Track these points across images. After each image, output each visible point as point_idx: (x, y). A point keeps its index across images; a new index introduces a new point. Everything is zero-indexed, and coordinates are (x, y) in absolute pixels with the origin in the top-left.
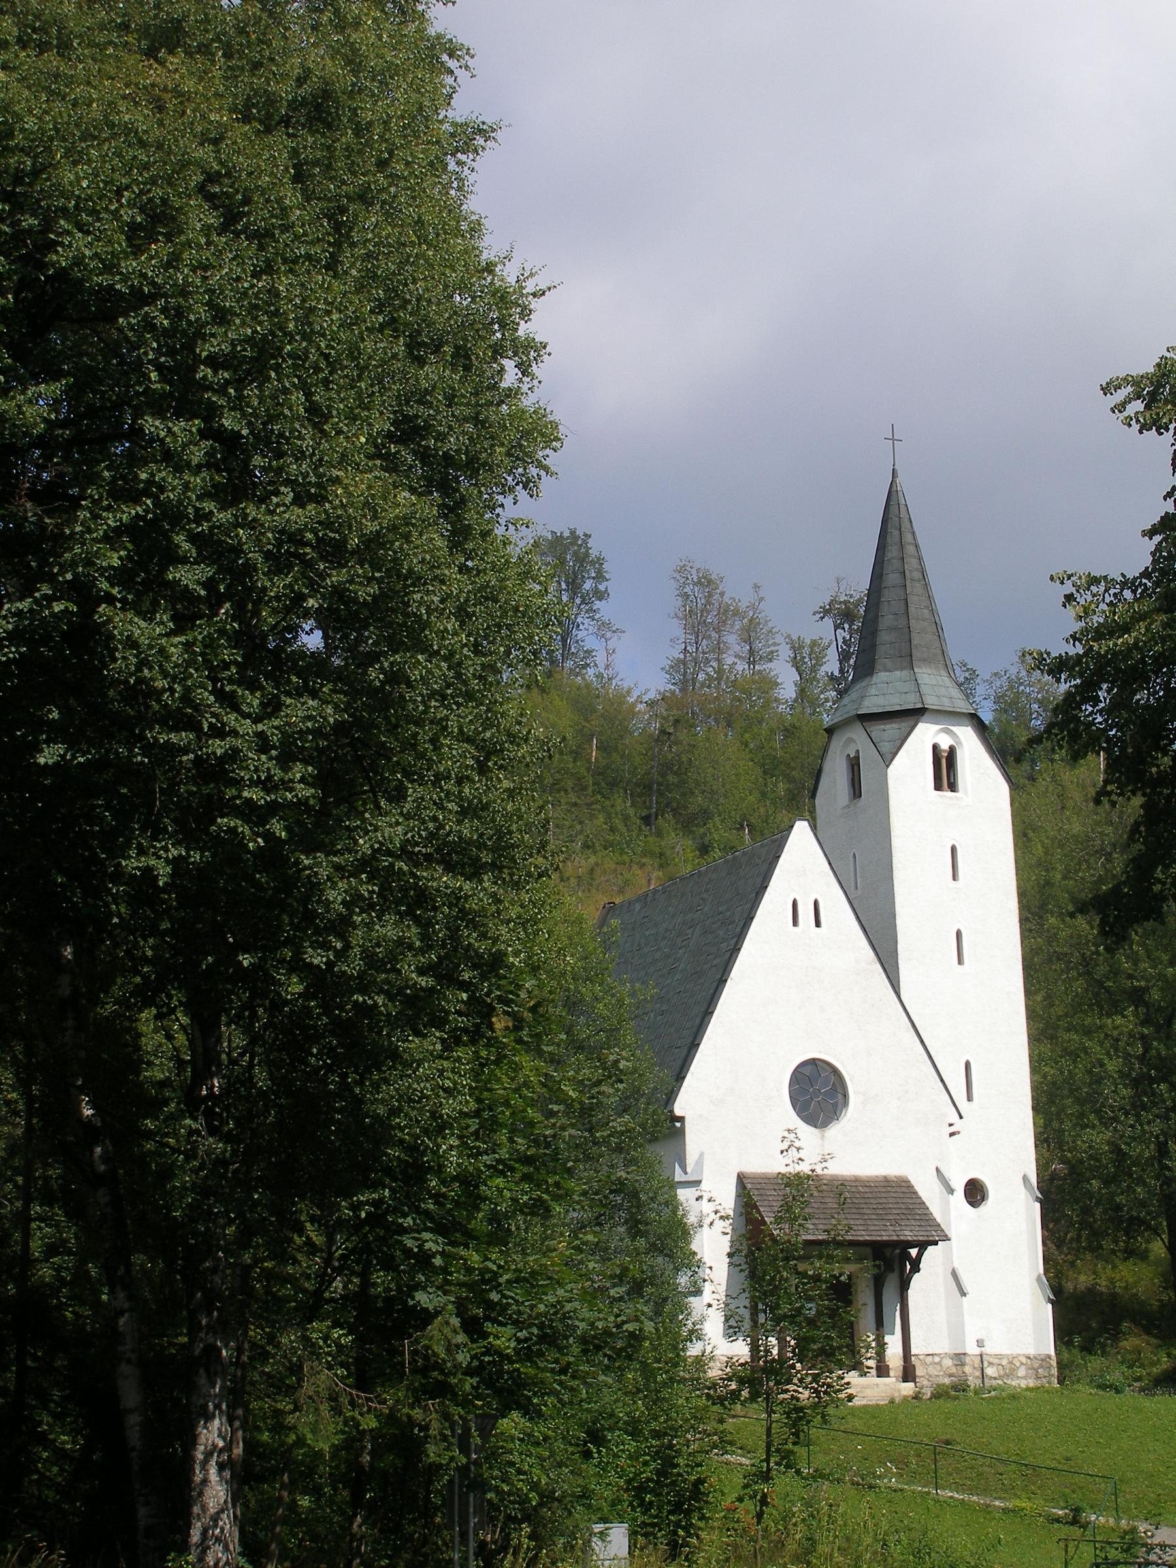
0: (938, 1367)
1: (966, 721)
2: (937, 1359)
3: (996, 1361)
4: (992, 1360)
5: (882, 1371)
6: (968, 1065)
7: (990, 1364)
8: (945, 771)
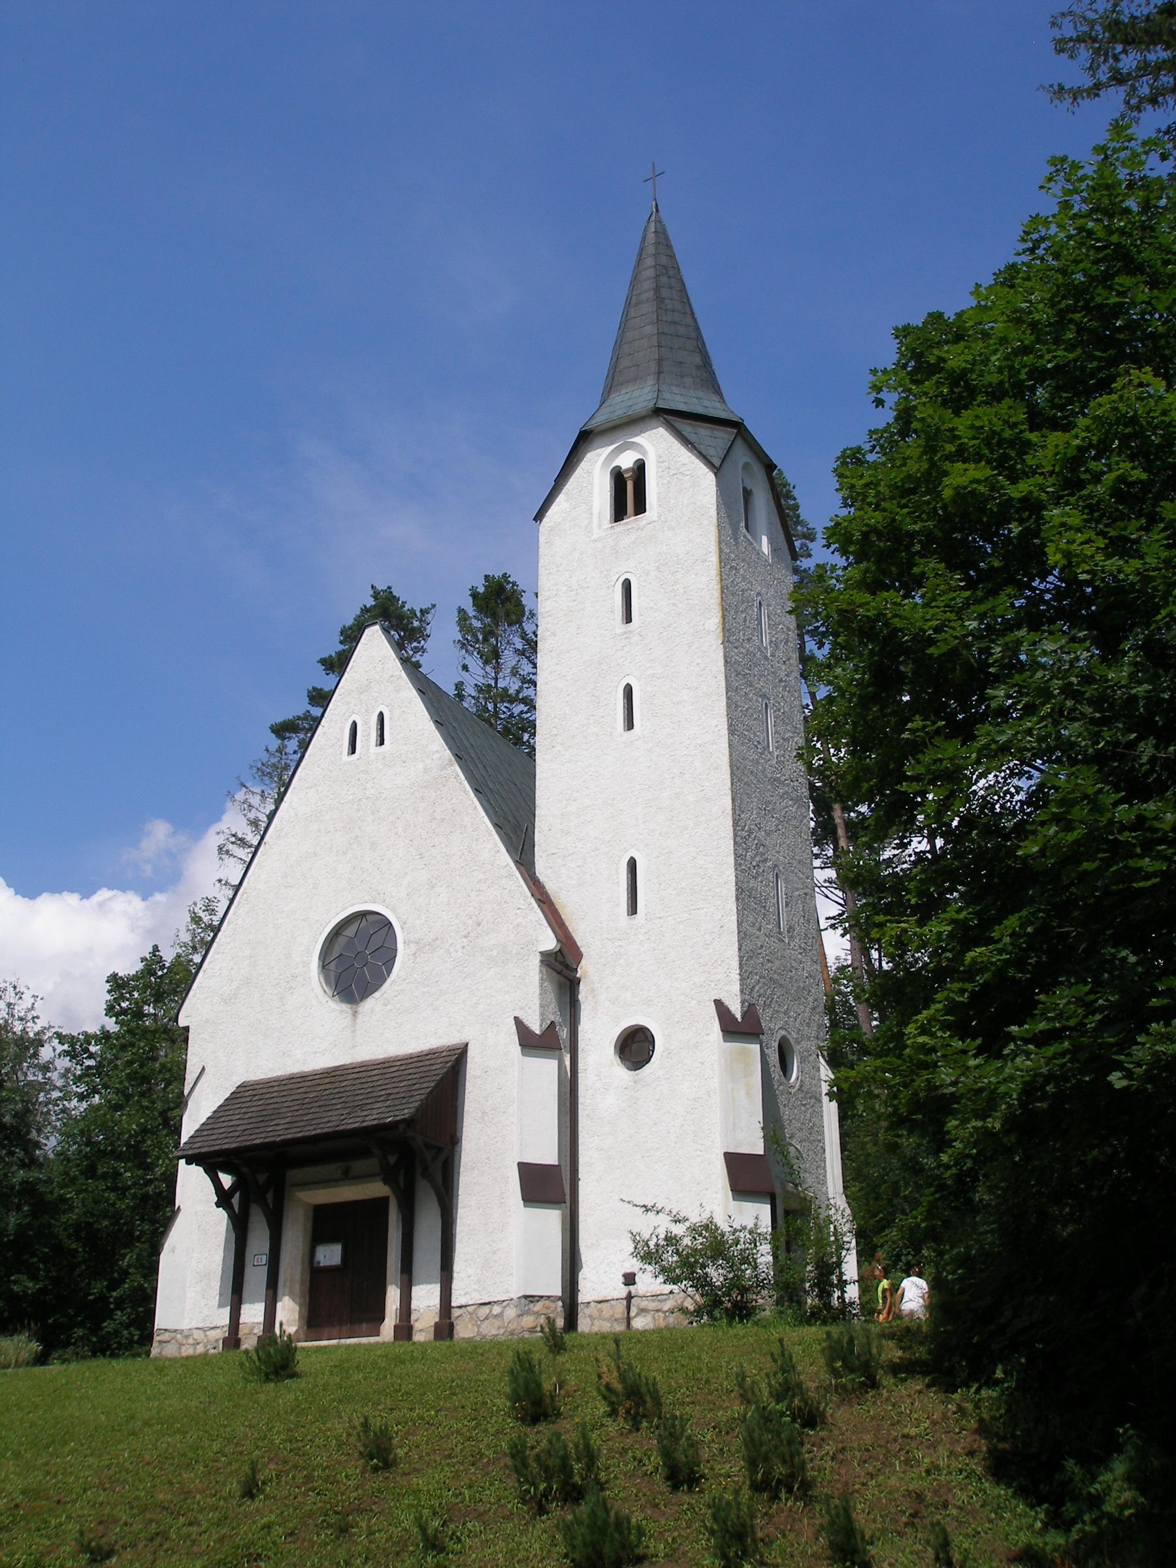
0: (497, 1323)
1: (654, 422)
2: (497, 1309)
3: (652, 1305)
4: (644, 1304)
5: (404, 1330)
6: (632, 865)
7: (643, 1311)
8: (629, 493)
